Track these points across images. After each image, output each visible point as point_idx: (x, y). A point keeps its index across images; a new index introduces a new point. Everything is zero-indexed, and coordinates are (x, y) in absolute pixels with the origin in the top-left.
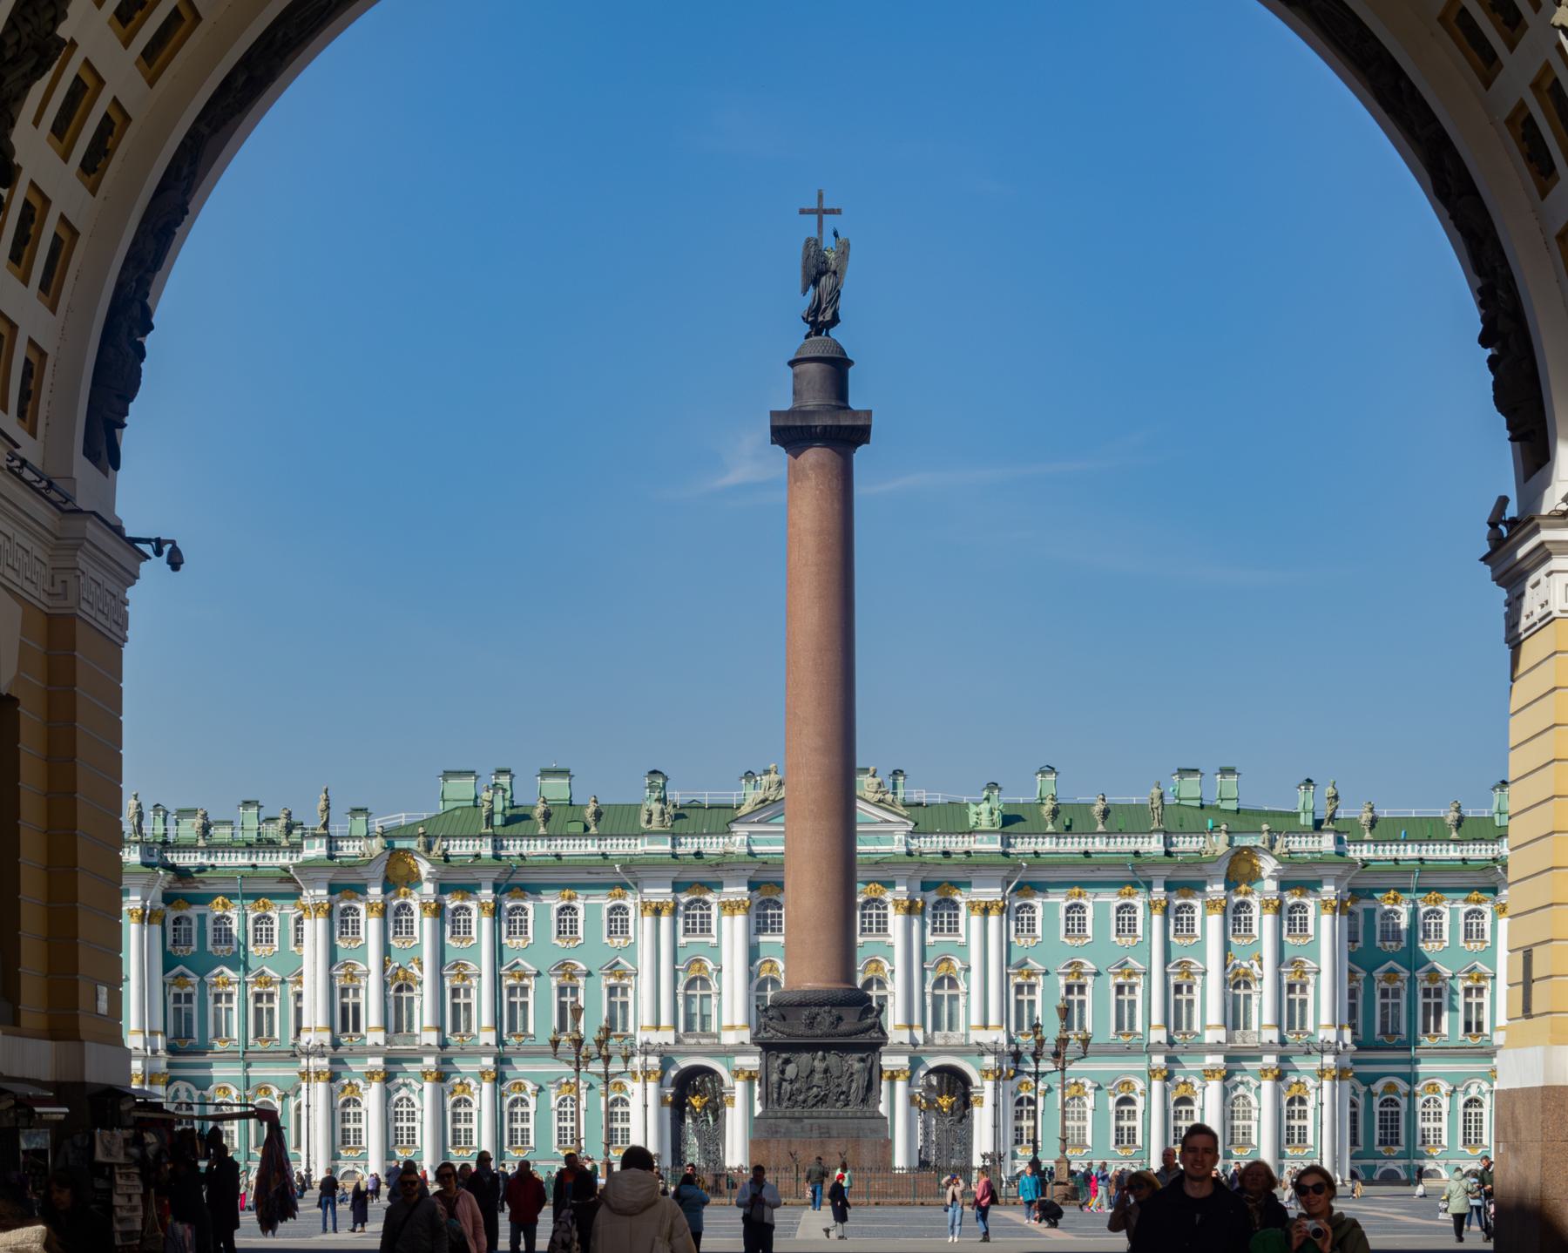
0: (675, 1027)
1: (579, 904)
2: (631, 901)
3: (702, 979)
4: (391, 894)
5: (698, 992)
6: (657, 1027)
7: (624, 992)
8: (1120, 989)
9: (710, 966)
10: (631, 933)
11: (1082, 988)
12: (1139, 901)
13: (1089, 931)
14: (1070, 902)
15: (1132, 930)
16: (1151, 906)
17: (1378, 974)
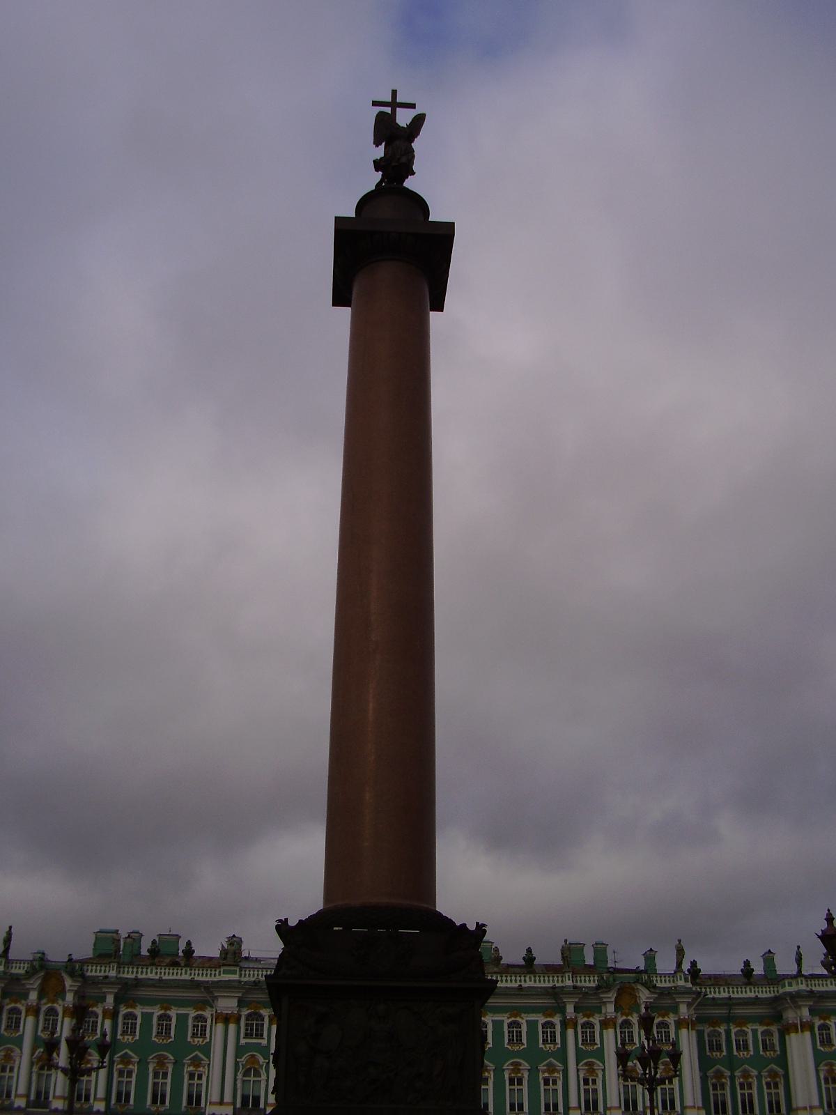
0: (234, 1103)
1: (173, 1013)
2: (207, 1013)
3: (255, 1070)
4: (44, 1001)
5: (252, 1079)
6: (221, 1103)
7: (200, 1077)
8: (546, 1082)
9: (261, 1060)
10: (208, 1035)
11: (520, 1082)
12: (556, 1020)
13: (524, 1040)
14: (510, 1020)
15: (553, 1041)
16: (565, 1024)
17: (710, 1073)
